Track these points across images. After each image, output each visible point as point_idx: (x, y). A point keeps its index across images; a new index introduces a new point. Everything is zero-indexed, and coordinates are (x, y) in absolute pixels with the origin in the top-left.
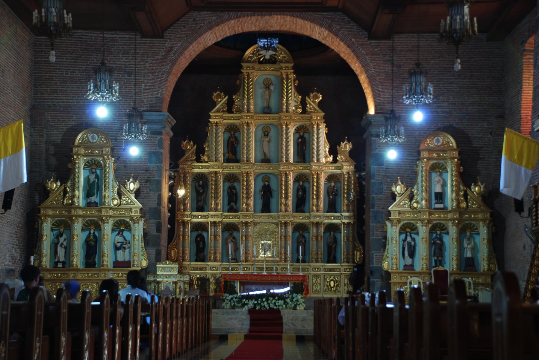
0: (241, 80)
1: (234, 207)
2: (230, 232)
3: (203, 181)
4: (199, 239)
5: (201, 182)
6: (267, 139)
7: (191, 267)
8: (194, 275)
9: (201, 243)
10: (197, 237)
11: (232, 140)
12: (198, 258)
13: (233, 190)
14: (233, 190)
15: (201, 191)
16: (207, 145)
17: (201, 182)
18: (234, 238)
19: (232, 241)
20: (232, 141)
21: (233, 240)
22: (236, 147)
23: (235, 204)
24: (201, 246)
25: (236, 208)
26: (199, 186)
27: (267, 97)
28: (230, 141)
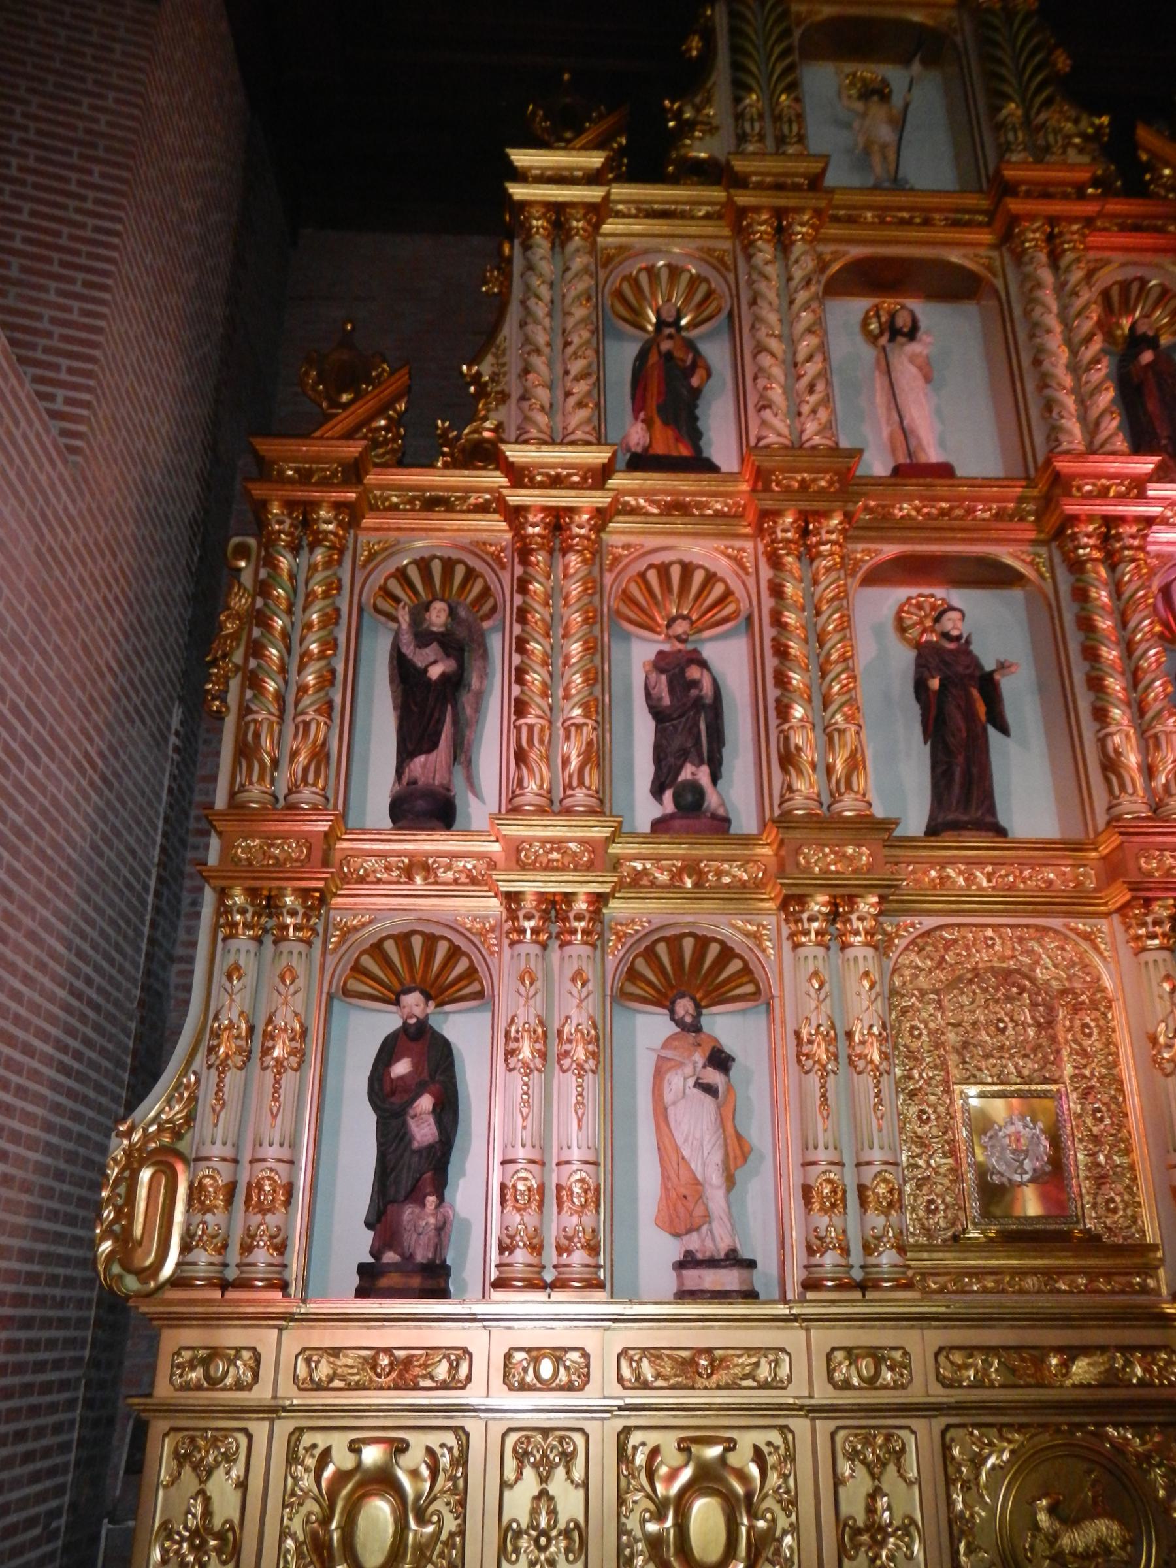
0: (708, 37)
1: (712, 800)
2: (684, 1007)
3: (452, 612)
4: (401, 1068)
5: (438, 616)
6: (914, 348)
7: (308, 1354)
8: (339, 1443)
9: (425, 1102)
10: (388, 1052)
11: (666, 346)
12: (390, 1257)
13: (694, 672)
14: (694, 672)
15: (435, 672)
16: (486, 368)
17: (438, 616)
18: (720, 1060)
19: (709, 1089)
20: (669, 356)
21: (713, 1076)
22: (696, 393)
23: (715, 778)
24: (423, 1131)
25: (721, 812)
26: (423, 638)
27: (885, 133)
28: (653, 358)
